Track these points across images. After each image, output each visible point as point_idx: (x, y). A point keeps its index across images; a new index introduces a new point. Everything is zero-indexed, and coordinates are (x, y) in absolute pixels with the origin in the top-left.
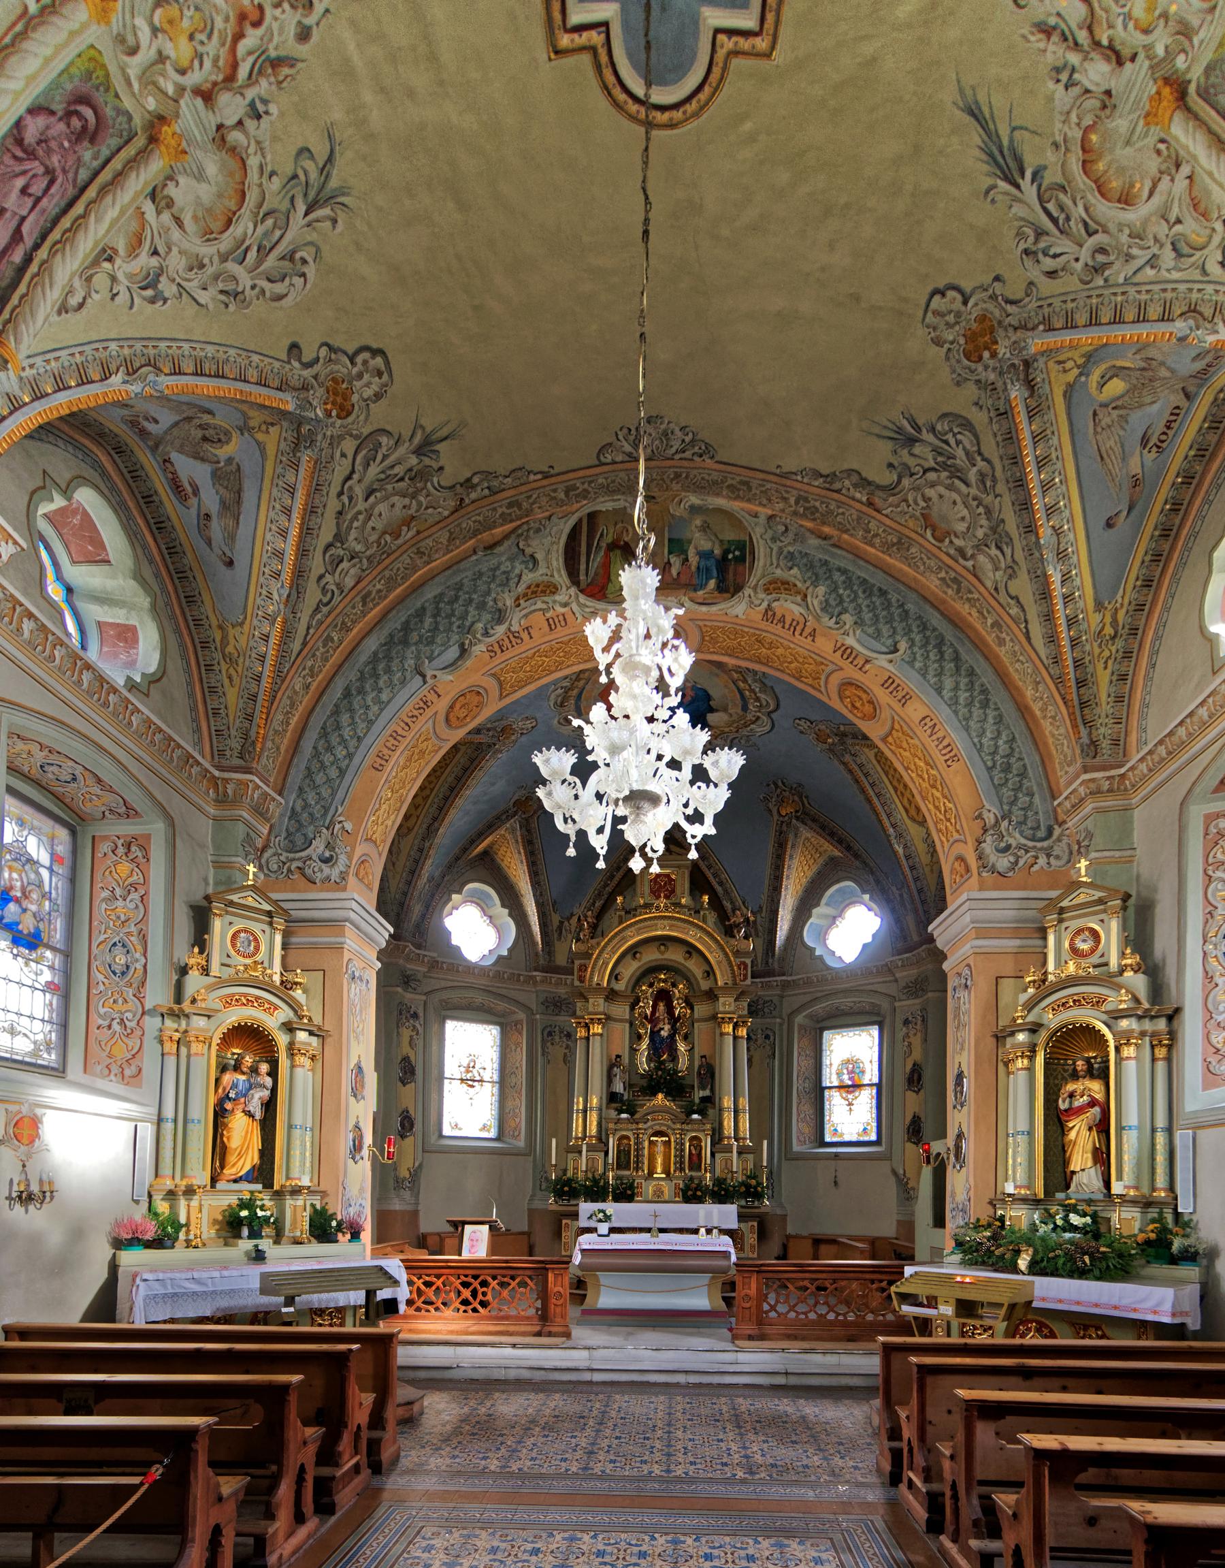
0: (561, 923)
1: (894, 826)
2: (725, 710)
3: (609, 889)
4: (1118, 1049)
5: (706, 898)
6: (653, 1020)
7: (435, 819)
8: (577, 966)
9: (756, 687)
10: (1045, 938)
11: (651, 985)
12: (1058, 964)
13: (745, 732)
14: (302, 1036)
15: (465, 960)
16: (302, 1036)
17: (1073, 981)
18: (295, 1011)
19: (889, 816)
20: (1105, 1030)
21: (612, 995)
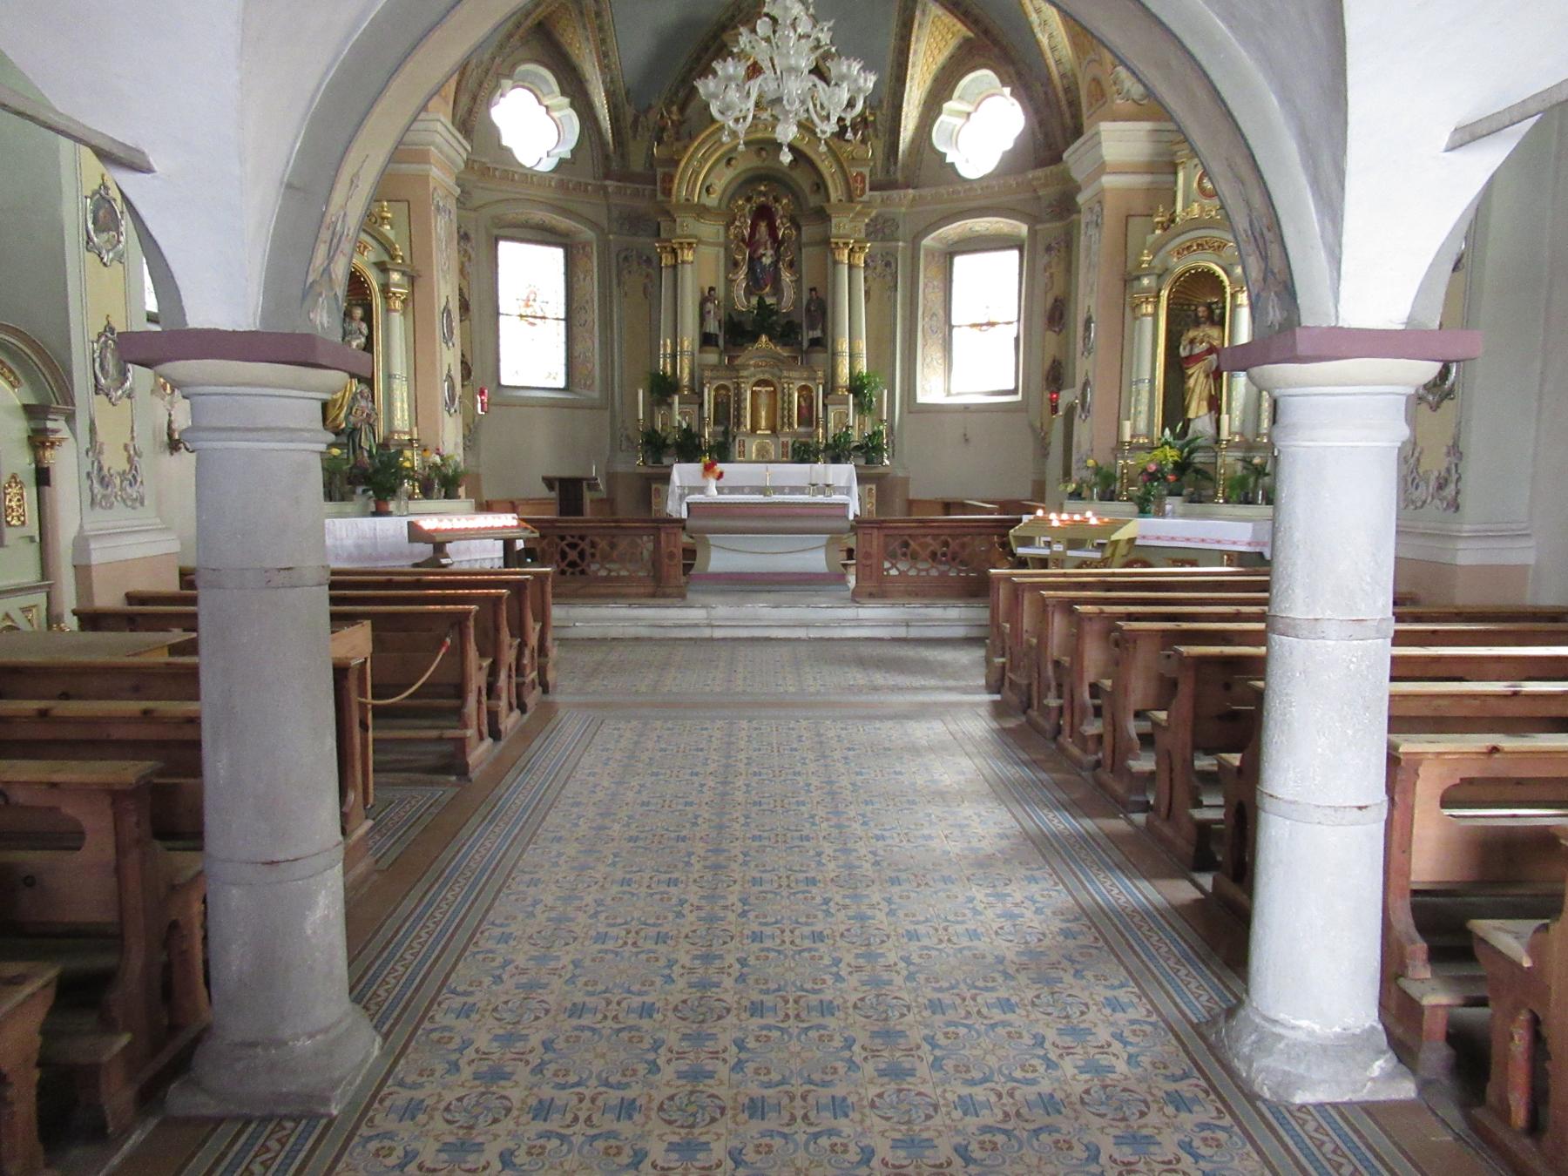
4: (1233, 296)
6: (751, 242)
8: (658, 177)
10: (1176, 174)
11: (749, 200)
12: (1186, 206)
14: (395, 277)
15: (522, 166)
16: (395, 277)
17: (1196, 224)
18: (387, 250)
20: (1224, 277)
21: (701, 211)
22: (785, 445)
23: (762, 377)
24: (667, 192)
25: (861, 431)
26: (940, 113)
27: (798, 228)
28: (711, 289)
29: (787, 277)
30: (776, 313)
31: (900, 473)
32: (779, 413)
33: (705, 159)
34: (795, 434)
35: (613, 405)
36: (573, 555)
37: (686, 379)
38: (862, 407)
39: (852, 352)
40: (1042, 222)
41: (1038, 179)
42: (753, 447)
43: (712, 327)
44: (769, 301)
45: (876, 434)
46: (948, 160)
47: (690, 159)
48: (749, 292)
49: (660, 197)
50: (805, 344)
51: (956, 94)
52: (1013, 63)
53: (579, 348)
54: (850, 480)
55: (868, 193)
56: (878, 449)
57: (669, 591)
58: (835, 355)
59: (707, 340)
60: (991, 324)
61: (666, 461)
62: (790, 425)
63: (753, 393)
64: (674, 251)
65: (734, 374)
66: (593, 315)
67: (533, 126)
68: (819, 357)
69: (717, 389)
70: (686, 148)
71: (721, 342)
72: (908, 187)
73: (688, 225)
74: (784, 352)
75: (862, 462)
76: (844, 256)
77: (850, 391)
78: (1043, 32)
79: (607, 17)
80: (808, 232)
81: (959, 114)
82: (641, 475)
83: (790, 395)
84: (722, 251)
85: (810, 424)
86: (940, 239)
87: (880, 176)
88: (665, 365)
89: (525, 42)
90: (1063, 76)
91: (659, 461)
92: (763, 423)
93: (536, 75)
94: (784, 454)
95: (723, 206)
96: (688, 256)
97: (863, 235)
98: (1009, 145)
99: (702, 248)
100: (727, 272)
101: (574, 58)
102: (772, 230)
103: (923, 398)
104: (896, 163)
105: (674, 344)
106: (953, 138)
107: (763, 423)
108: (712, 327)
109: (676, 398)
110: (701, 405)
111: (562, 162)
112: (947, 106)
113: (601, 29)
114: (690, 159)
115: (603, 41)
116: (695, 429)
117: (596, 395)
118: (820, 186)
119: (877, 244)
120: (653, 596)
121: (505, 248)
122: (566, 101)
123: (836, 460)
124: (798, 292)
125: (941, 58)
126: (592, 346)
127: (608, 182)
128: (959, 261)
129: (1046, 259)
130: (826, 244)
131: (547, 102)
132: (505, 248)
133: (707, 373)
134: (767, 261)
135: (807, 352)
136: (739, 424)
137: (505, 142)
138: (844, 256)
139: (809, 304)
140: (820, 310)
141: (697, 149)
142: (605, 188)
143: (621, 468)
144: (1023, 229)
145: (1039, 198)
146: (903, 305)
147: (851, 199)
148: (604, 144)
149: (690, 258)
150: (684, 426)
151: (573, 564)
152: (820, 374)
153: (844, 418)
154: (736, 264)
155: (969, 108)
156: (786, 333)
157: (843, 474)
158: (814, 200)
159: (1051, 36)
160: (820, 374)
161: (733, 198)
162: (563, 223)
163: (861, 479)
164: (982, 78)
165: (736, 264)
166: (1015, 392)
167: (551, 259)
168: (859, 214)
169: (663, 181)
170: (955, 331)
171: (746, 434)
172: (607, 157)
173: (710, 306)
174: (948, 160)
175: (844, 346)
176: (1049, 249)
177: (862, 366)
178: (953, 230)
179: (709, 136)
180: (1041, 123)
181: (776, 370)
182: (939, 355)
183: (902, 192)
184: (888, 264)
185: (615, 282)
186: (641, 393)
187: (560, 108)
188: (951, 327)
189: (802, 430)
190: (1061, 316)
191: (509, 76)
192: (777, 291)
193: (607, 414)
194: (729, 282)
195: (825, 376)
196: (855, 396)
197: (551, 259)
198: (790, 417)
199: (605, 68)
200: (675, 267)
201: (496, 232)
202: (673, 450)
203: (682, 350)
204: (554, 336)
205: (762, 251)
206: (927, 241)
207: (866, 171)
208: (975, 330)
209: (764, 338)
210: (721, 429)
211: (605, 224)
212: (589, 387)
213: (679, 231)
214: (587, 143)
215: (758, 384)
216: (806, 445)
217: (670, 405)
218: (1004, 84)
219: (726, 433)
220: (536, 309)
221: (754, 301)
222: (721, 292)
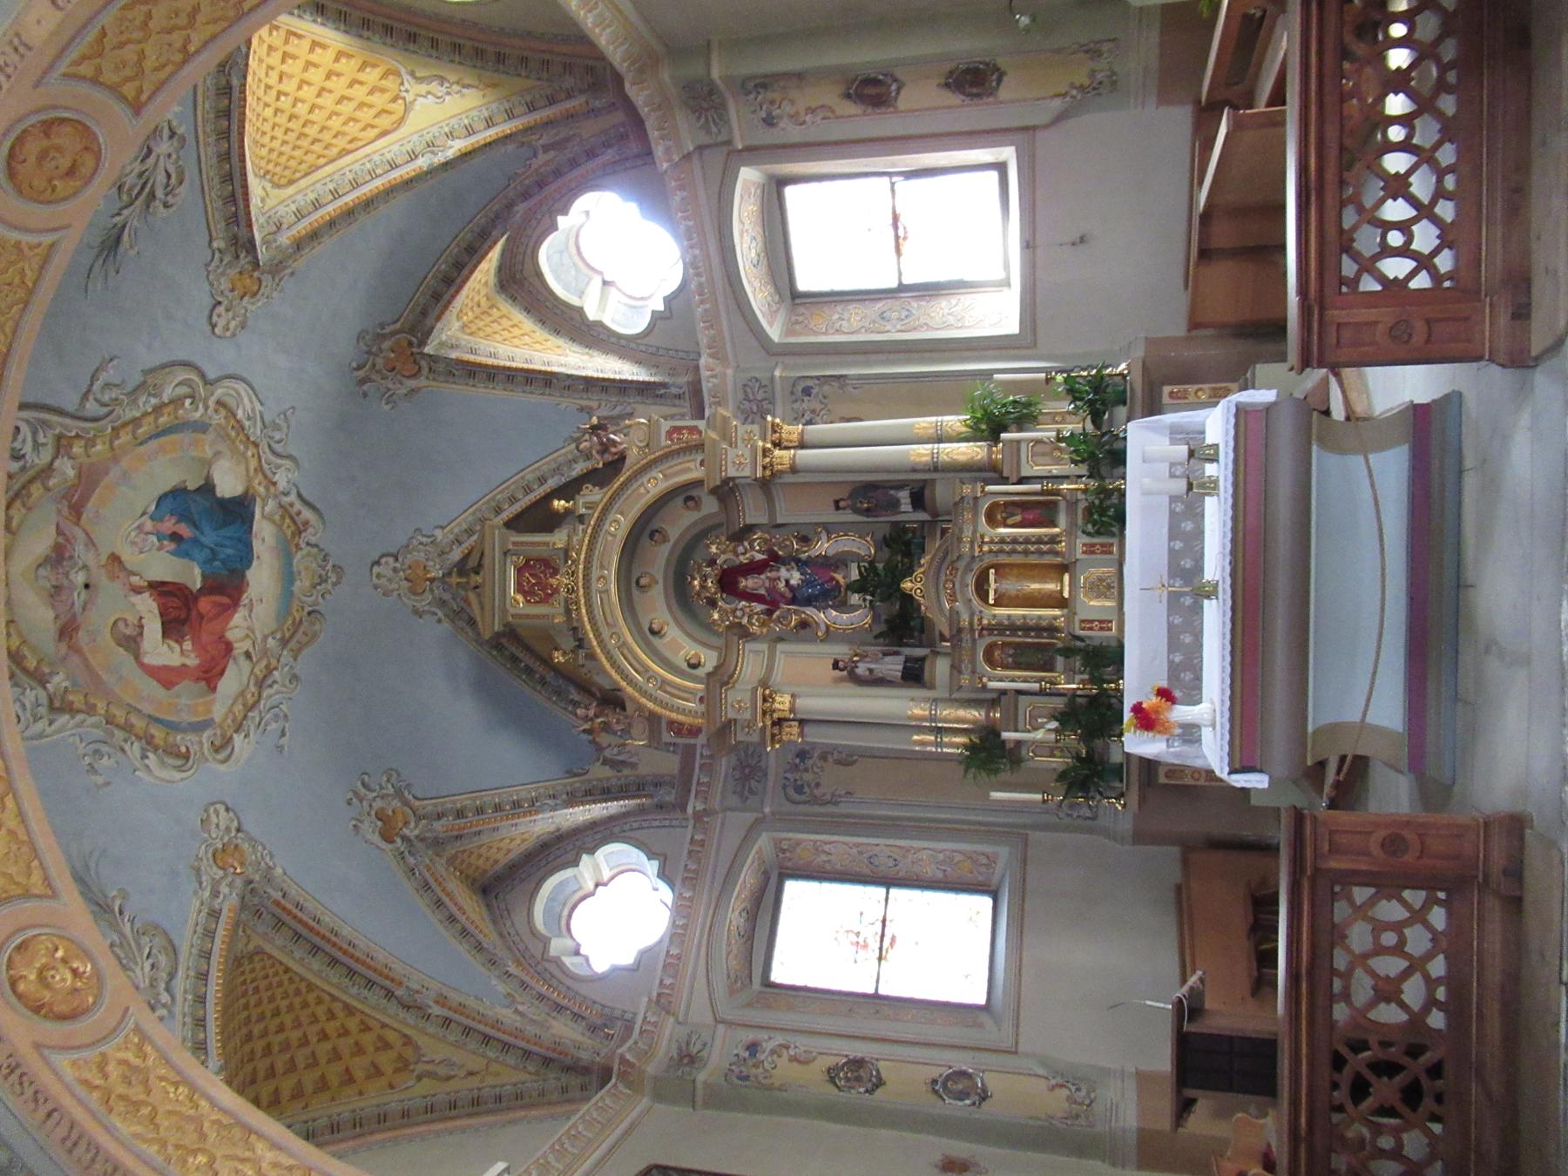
0: (606, 762)
1: (413, 156)
2: (208, 464)
3: (550, 676)
5: (556, 504)
6: (771, 602)
7: (389, 994)
9: (147, 403)
11: (712, 603)
13: (255, 432)
19: (393, 166)
21: (721, 678)
22: (1090, 549)
23: (971, 589)
24: (694, 731)
25: (1064, 417)
26: (600, 324)
27: (750, 529)
28: (836, 666)
29: (823, 547)
30: (871, 563)
31: (1139, 353)
32: (1033, 560)
33: (644, 671)
34: (1070, 532)
35: (1025, 826)
36: (1385, 1090)
37: (975, 714)
38: (1025, 417)
39: (933, 439)
40: (729, 142)
41: (668, 150)
42: (1094, 606)
43: (893, 666)
44: (855, 575)
45: (1073, 392)
46: (661, 308)
47: (644, 693)
48: (843, 606)
49: (701, 739)
50: (923, 516)
51: (573, 300)
52: (510, 206)
53: (930, 871)
54: (1156, 429)
55: (701, 424)
56: (1098, 384)
57: (1498, 859)
58: (936, 467)
59: (914, 675)
60: (896, 218)
61: (1116, 758)
62: (1053, 540)
63: (997, 604)
64: (779, 722)
65: (966, 637)
66: (882, 846)
67: (617, 913)
68: (942, 494)
69: (993, 664)
70: (633, 700)
71: (919, 652)
72: (697, 368)
73: (738, 700)
74: (934, 545)
75: (1122, 411)
76: (783, 456)
77: (995, 439)
78: (445, 148)
79: (464, 801)
80: (752, 512)
81: (603, 297)
82: (1143, 799)
83: (1002, 541)
84: (780, 647)
85: (1055, 503)
86: (773, 315)
87: (686, 407)
88: (955, 745)
89: (498, 916)
90: (510, 115)
91: (1117, 771)
92: (1051, 586)
93: (551, 899)
94: (1106, 549)
95: (720, 642)
96: (782, 703)
97: (756, 428)
98: (632, 208)
99: (777, 677)
100: (813, 639)
101: (524, 847)
102: (755, 568)
103: (1010, 324)
104: (663, 385)
105: (920, 729)
106: (635, 302)
107: (1051, 586)
108: (893, 666)
109: (1006, 735)
110: (1019, 692)
111: (663, 875)
112: (592, 314)
113: (480, 811)
114: (644, 693)
115: (498, 808)
116: (1059, 703)
117: (1003, 852)
118: (686, 493)
119: (779, 409)
120: (1515, 904)
121: (778, 975)
122: (585, 857)
123: (1118, 458)
124: (845, 528)
125: (528, 324)
126: (926, 852)
127: (690, 810)
128: (803, 285)
129: (782, 125)
130: (767, 484)
131: (590, 885)
132: (778, 975)
133: (965, 680)
134: (796, 578)
135: (935, 514)
136: (1052, 630)
137: (627, 958)
138: (783, 456)
139: (857, 511)
140: (868, 493)
141: (631, 682)
142: (698, 816)
143: (1126, 825)
144: (749, 176)
145: (700, 148)
146: (868, 364)
147: (700, 447)
148: (641, 810)
149: (787, 699)
150: (1054, 725)
151: (1412, 1095)
152: (967, 490)
153: (1044, 451)
154: (804, 625)
155: (596, 282)
156: (903, 547)
157: (1148, 444)
158: (710, 506)
159: (450, 135)
160: (967, 490)
161: (709, 627)
162: (747, 878)
163: (1153, 407)
164: (548, 256)
165: (804, 625)
166: (1001, 168)
167: (803, 901)
168: (726, 435)
169: (679, 733)
170: (906, 281)
171: (1069, 619)
172: (660, 807)
173: (861, 670)
174: (661, 308)
175: (921, 453)
176: (769, 122)
177: (955, 421)
178: (757, 293)
179: (614, 664)
180: (591, 154)
181: (961, 565)
182: (944, 303)
183: (705, 374)
184: (807, 392)
185: (831, 809)
186: (996, 795)
187: (597, 867)
188: (902, 288)
189: (1062, 519)
190: (874, 82)
191: (546, 942)
192: (839, 562)
193: (1035, 836)
194: (830, 635)
195: (975, 480)
196: (1005, 430)
197: (803, 901)
198: (1039, 541)
199: (534, 806)
200: (802, 722)
201: (757, 979)
202: (1098, 743)
203: (929, 717)
204: (914, 908)
205: (781, 585)
206: (774, 333)
207: (666, 426)
208: (904, 249)
209: (907, 585)
210: (1060, 660)
211: (750, 817)
212: (991, 860)
213: (747, 715)
214: (637, 834)
215: (982, 594)
216: (1089, 511)
217: (1019, 743)
218: (553, 227)
219: (1068, 652)
220: (871, 934)
221: (855, 599)
222: (842, 651)
